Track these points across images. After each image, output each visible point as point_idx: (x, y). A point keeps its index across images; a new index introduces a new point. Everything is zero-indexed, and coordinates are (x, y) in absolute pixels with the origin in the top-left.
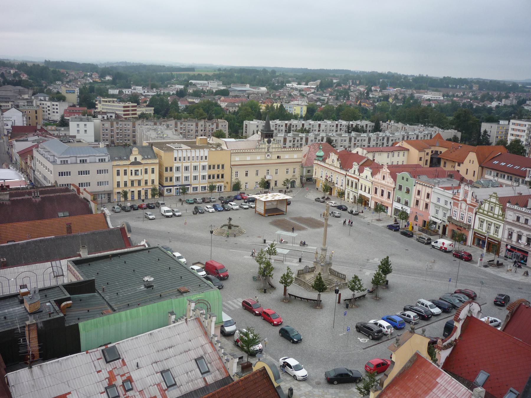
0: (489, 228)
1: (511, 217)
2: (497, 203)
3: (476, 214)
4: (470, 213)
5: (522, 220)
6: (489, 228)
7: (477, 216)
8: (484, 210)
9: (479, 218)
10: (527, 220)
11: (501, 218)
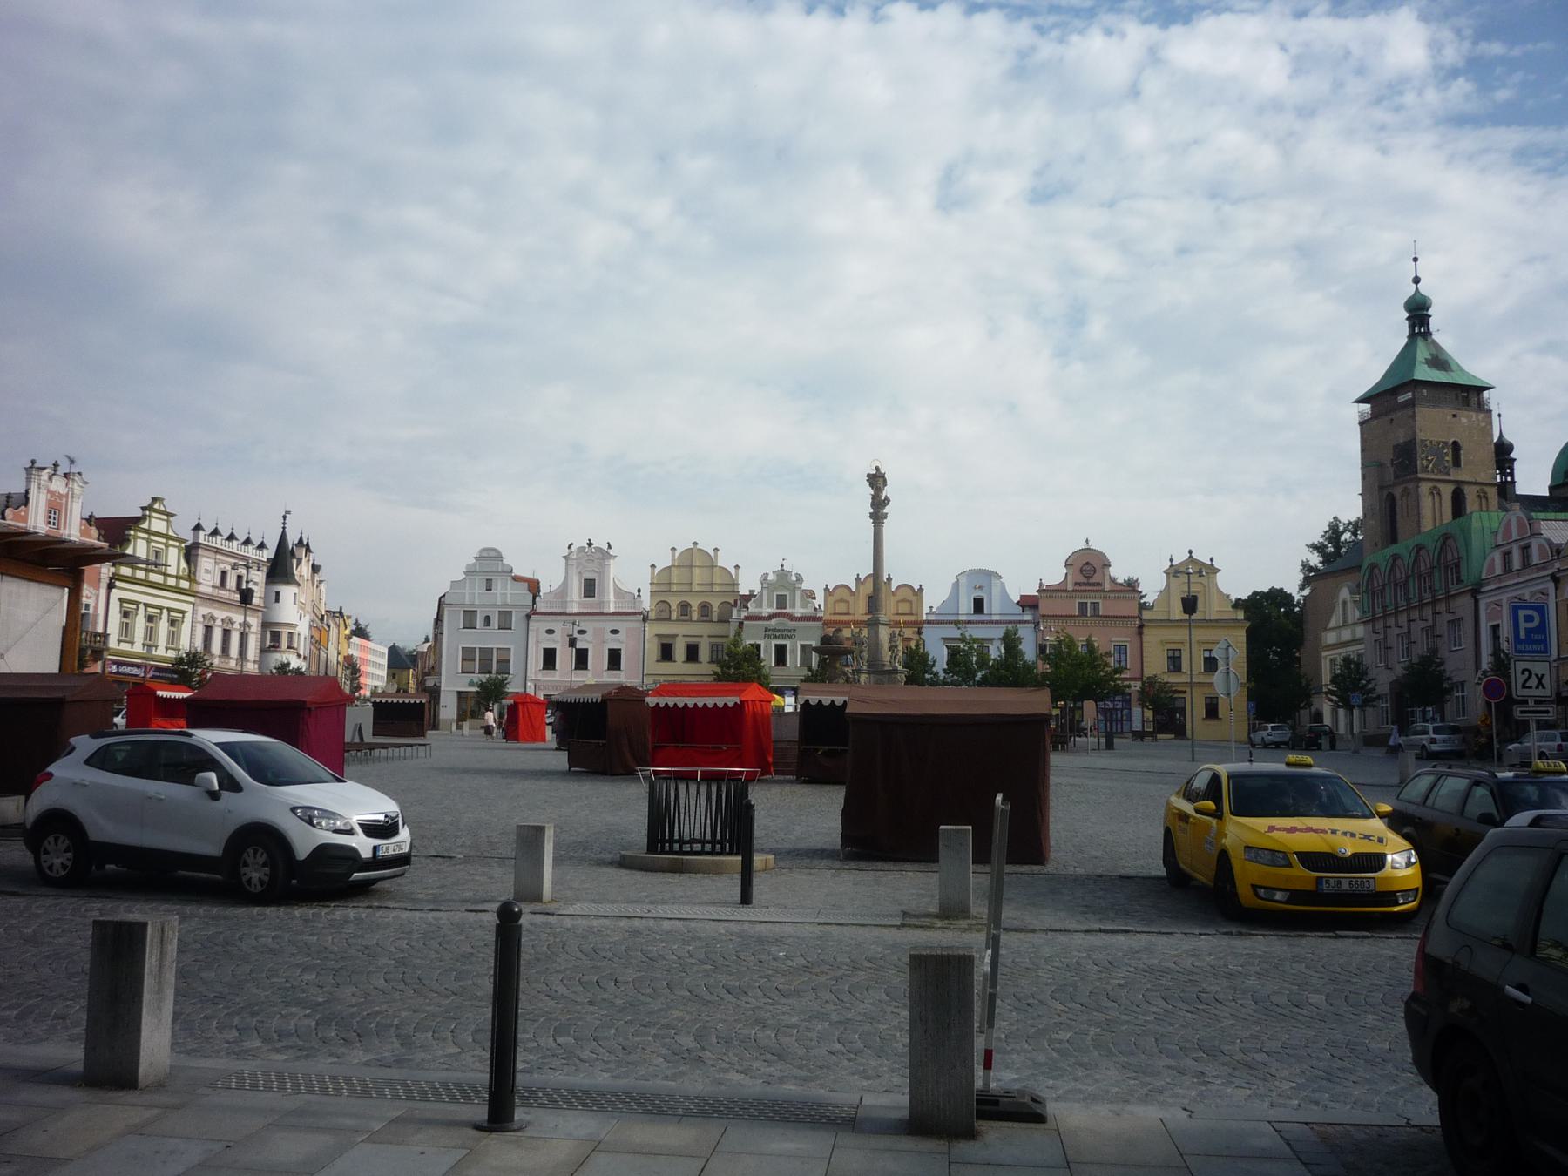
0: (150, 634)
1: (207, 577)
2: (171, 533)
3: (111, 586)
6: (150, 634)
7: (115, 594)
9: (122, 600)
11: (185, 584)
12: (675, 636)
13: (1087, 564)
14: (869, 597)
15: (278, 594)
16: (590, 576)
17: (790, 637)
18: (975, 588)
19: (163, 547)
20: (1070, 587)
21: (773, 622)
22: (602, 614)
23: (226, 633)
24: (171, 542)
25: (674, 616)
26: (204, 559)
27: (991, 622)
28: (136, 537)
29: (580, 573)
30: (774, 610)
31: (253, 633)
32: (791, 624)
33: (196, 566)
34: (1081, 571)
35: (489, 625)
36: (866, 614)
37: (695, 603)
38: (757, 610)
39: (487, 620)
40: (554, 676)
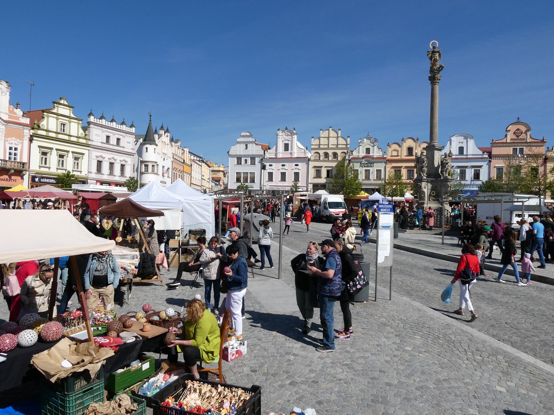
1: (98, 138)
2: (72, 115)
3: (31, 140)
4: (13, 142)
5: (113, 141)
7: (36, 143)
8: (47, 131)
10: (118, 140)
12: (321, 167)
13: (518, 129)
14: (408, 148)
15: (147, 148)
16: (287, 142)
17: (371, 167)
18: (460, 142)
19: (68, 122)
20: (509, 141)
21: (364, 161)
22: (291, 158)
23: (112, 164)
24: (72, 120)
25: (322, 158)
26: (94, 129)
27: (467, 158)
28: (48, 117)
29: (282, 141)
30: (364, 154)
31: (128, 165)
32: (372, 160)
33: (89, 132)
34: (514, 133)
35: (246, 163)
36: (406, 156)
37: (330, 152)
38: (357, 155)
39: (246, 160)
40: (285, 184)
